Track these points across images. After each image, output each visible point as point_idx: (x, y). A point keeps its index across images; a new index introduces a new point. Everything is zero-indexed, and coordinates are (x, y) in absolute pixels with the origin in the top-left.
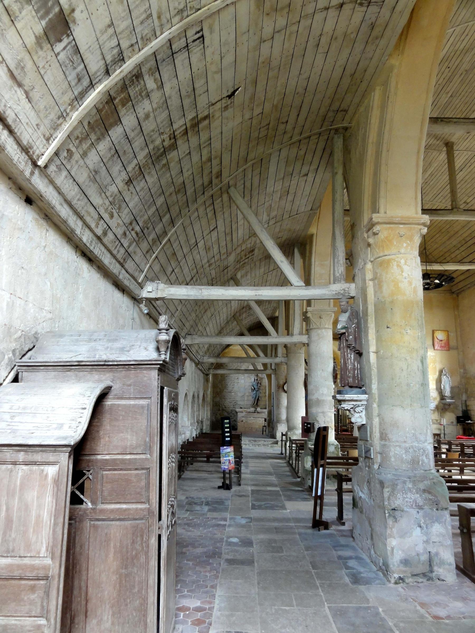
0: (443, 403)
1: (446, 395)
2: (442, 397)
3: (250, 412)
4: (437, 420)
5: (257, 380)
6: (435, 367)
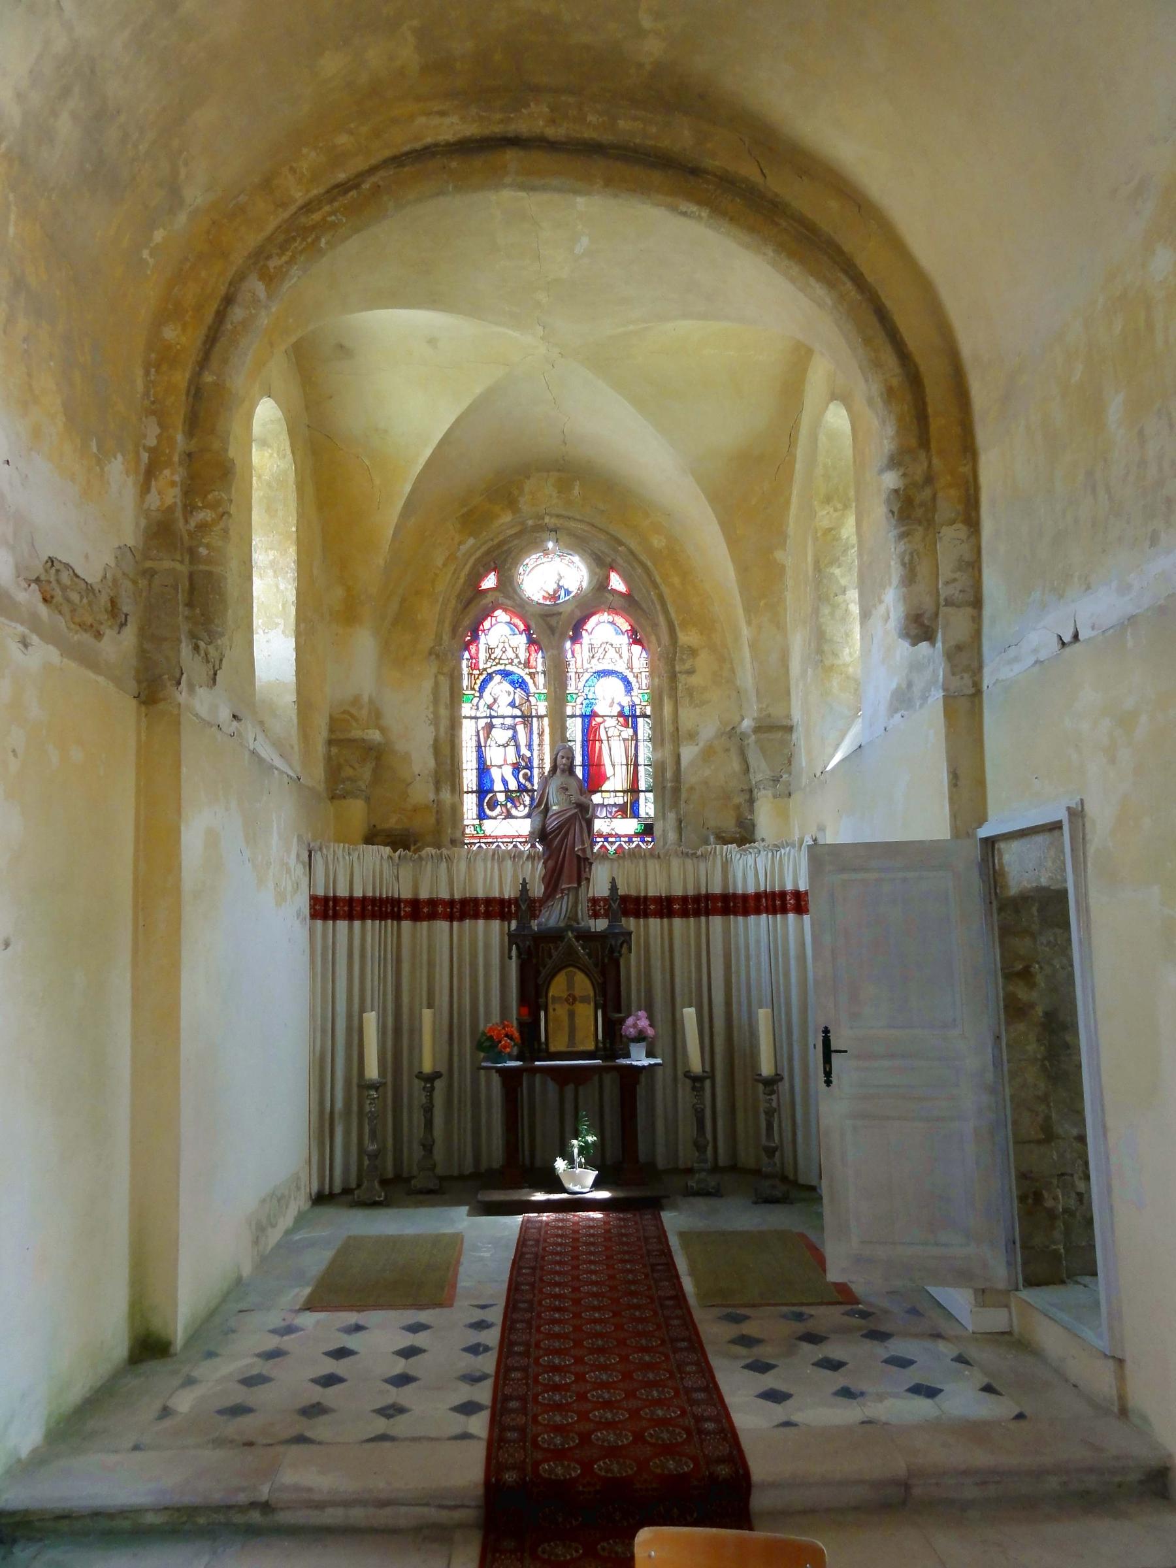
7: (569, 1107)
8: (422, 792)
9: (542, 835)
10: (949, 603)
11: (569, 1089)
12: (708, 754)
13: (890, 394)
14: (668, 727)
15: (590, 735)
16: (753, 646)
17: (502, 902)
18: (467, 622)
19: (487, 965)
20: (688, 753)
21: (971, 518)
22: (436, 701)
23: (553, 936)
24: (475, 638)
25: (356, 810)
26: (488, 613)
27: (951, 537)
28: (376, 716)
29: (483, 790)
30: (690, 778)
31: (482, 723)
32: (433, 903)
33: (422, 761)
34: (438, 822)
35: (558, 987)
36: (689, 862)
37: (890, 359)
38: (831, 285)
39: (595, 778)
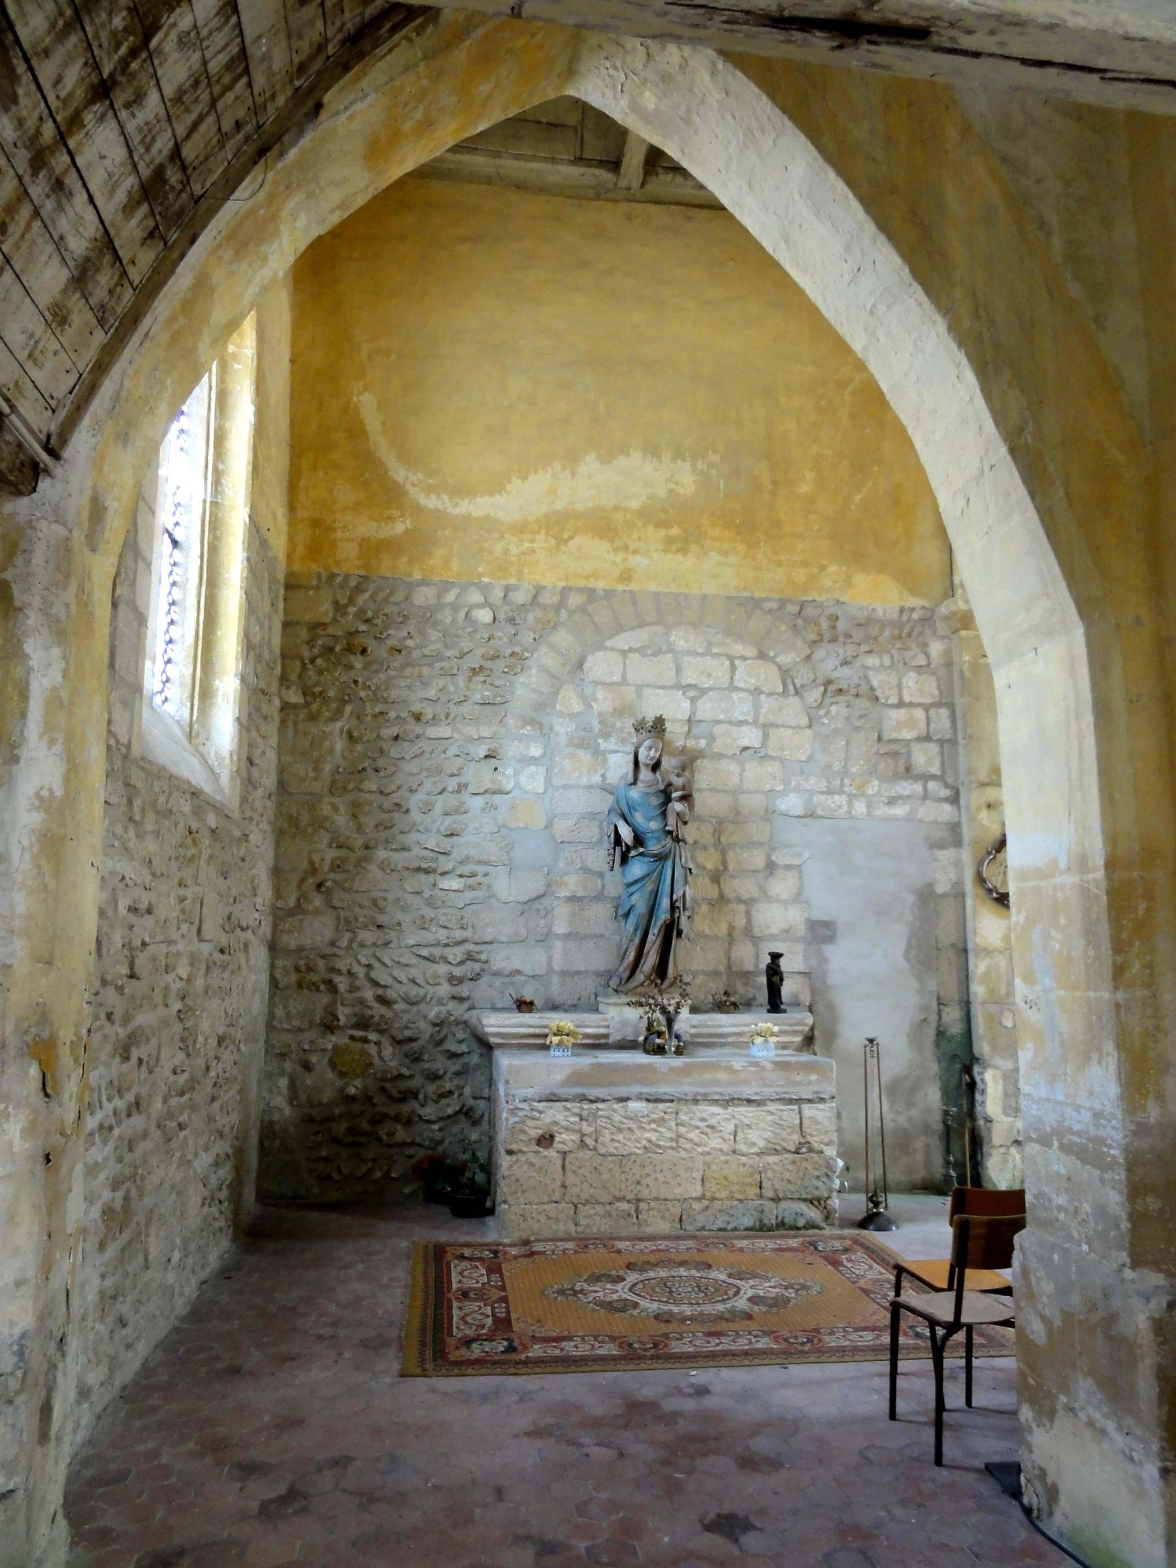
3: (599, 1044)
5: (656, 767)
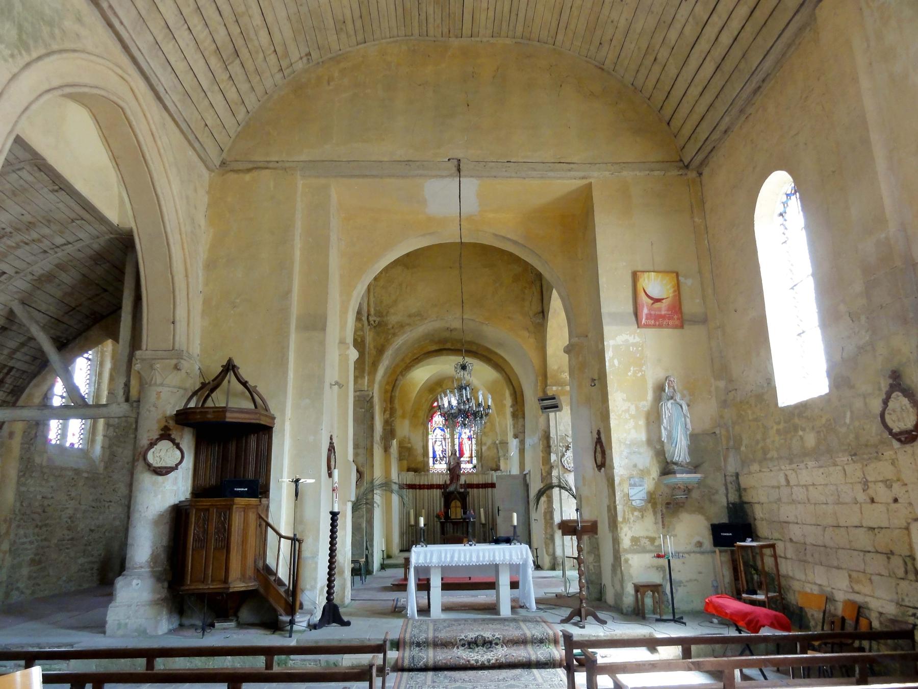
0: (667, 485)
1: (676, 459)
2: (667, 468)
4: (652, 540)
6: (643, 376)
7: (455, 530)
8: (420, 458)
9: (449, 469)
10: (520, 432)
11: (455, 527)
12: (489, 448)
13: (511, 395)
14: (480, 442)
15: (461, 445)
16: (499, 423)
17: (440, 485)
18: (430, 415)
19: (436, 500)
20: (484, 448)
21: (524, 418)
22: (423, 436)
23: (452, 493)
24: (432, 419)
25: (405, 462)
26: (435, 412)
27: (521, 420)
28: (409, 439)
29: (434, 457)
30: (485, 454)
31: (434, 440)
32: (424, 485)
33: (420, 451)
34: (424, 465)
35: (453, 504)
36: (484, 476)
37: (511, 387)
38: (501, 373)
39: (462, 454)
